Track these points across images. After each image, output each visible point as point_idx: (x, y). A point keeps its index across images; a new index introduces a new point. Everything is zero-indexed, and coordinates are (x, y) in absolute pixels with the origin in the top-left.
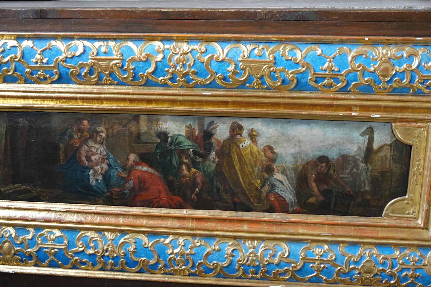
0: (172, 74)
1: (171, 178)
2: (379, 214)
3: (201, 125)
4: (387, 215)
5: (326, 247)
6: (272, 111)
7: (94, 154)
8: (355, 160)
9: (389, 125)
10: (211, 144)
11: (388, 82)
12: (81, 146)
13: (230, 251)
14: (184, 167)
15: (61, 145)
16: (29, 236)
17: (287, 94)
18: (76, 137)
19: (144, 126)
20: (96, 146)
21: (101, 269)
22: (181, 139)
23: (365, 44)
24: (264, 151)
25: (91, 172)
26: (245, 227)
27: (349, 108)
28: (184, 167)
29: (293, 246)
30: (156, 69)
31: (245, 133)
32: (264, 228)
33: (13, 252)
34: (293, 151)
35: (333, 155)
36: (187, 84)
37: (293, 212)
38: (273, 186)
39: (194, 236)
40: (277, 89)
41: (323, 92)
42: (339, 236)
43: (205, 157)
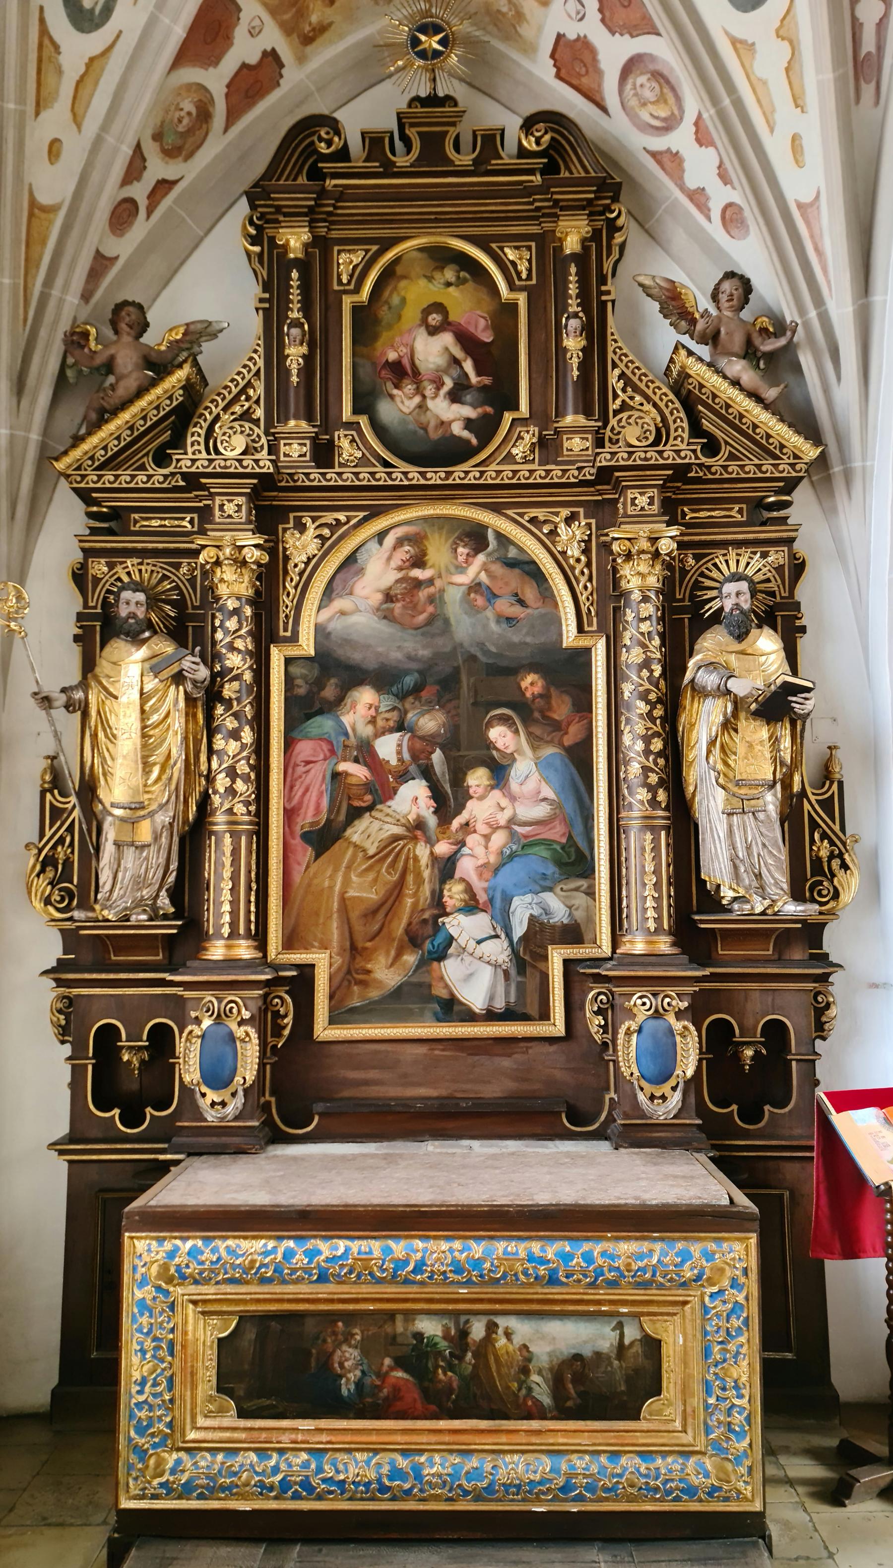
0: (432, 1271)
1: (426, 1384)
2: (636, 1417)
3: (457, 1323)
4: (645, 1419)
5: (587, 1457)
6: (525, 1307)
7: (347, 1360)
8: (609, 1358)
9: (637, 1320)
10: (467, 1344)
11: (633, 1277)
12: (334, 1351)
13: (489, 1469)
14: (440, 1371)
15: (314, 1351)
16: (273, 1463)
17: (540, 1290)
18: (329, 1340)
19: (400, 1327)
20: (351, 1350)
21: (351, 1499)
22: (437, 1340)
23: (608, 1239)
24: (520, 1349)
25: (343, 1381)
26: (504, 1439)
27: (599, 1302)
28: (440, 1371)
29: (555, 1458)
30: (415, 1268)
31: (500, 1331)
32: (522, 1438)
33: (253, 1483)
34: (548, 1349)
35: (587, 1352)
36: (445, 1282)
37: (552, 1418)
38: (530, 1390)
39: (451, 1451)
40: (531, 1285)
41: (573, 1287)
42: (600, 1445)
43: (461, 1358)
